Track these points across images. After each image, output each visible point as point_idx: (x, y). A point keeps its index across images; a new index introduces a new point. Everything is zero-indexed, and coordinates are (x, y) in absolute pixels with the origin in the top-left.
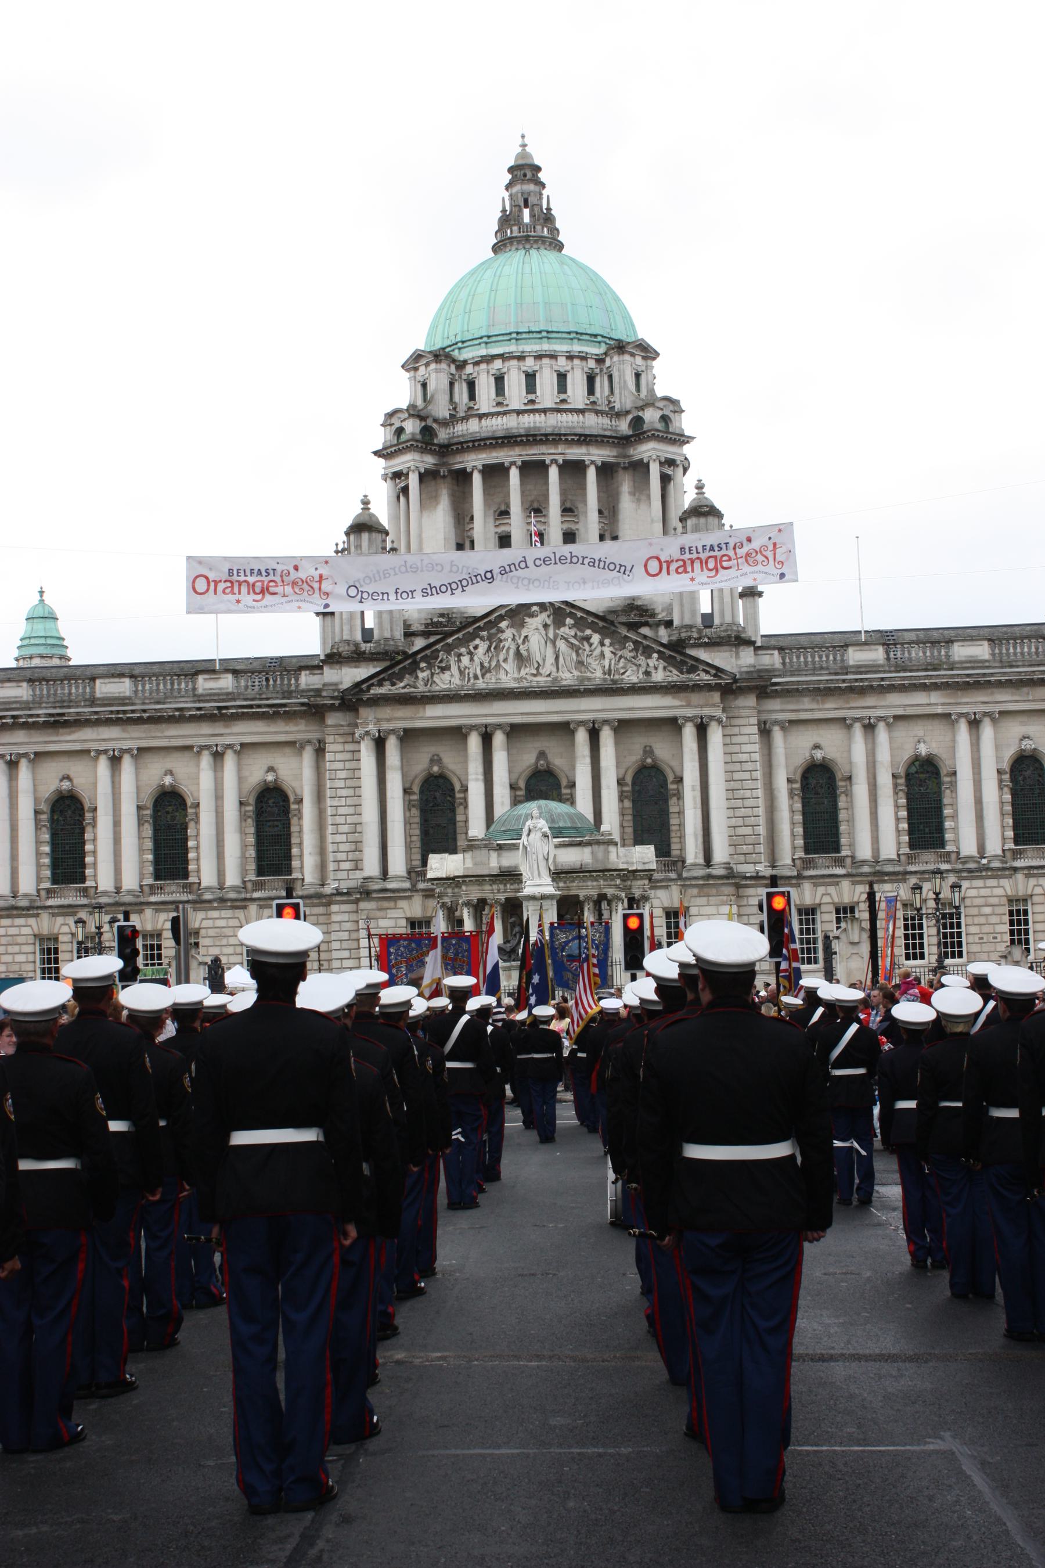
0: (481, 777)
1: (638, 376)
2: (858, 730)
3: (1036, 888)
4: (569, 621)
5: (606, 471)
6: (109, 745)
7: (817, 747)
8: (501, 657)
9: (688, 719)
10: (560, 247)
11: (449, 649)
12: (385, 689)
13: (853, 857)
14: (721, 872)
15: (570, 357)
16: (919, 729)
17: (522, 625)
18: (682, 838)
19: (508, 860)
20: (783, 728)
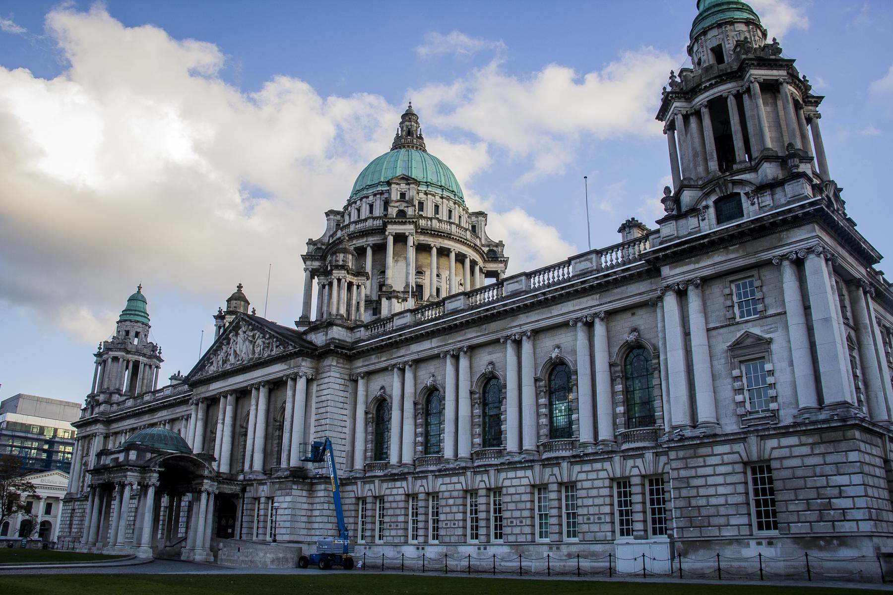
3: (505, 481)
6: (164, 418)
16: (432, 367)
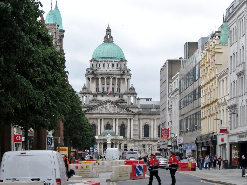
0: (100, 125)
1: (124, 65)
2: (152, 120)
4: (113, 104)
5: (119, 79)
7: (146, 122)
8: (103, 109)
9: (129, 118)
10: (113, 42)
11: (96, 107)
12: (87, 112)
13: (150, 138)
14: (132, 139)
15: (114, 62)
17: (106, 104)
18: (127, 134)
19: (104, 138)
20: (142, 119)
